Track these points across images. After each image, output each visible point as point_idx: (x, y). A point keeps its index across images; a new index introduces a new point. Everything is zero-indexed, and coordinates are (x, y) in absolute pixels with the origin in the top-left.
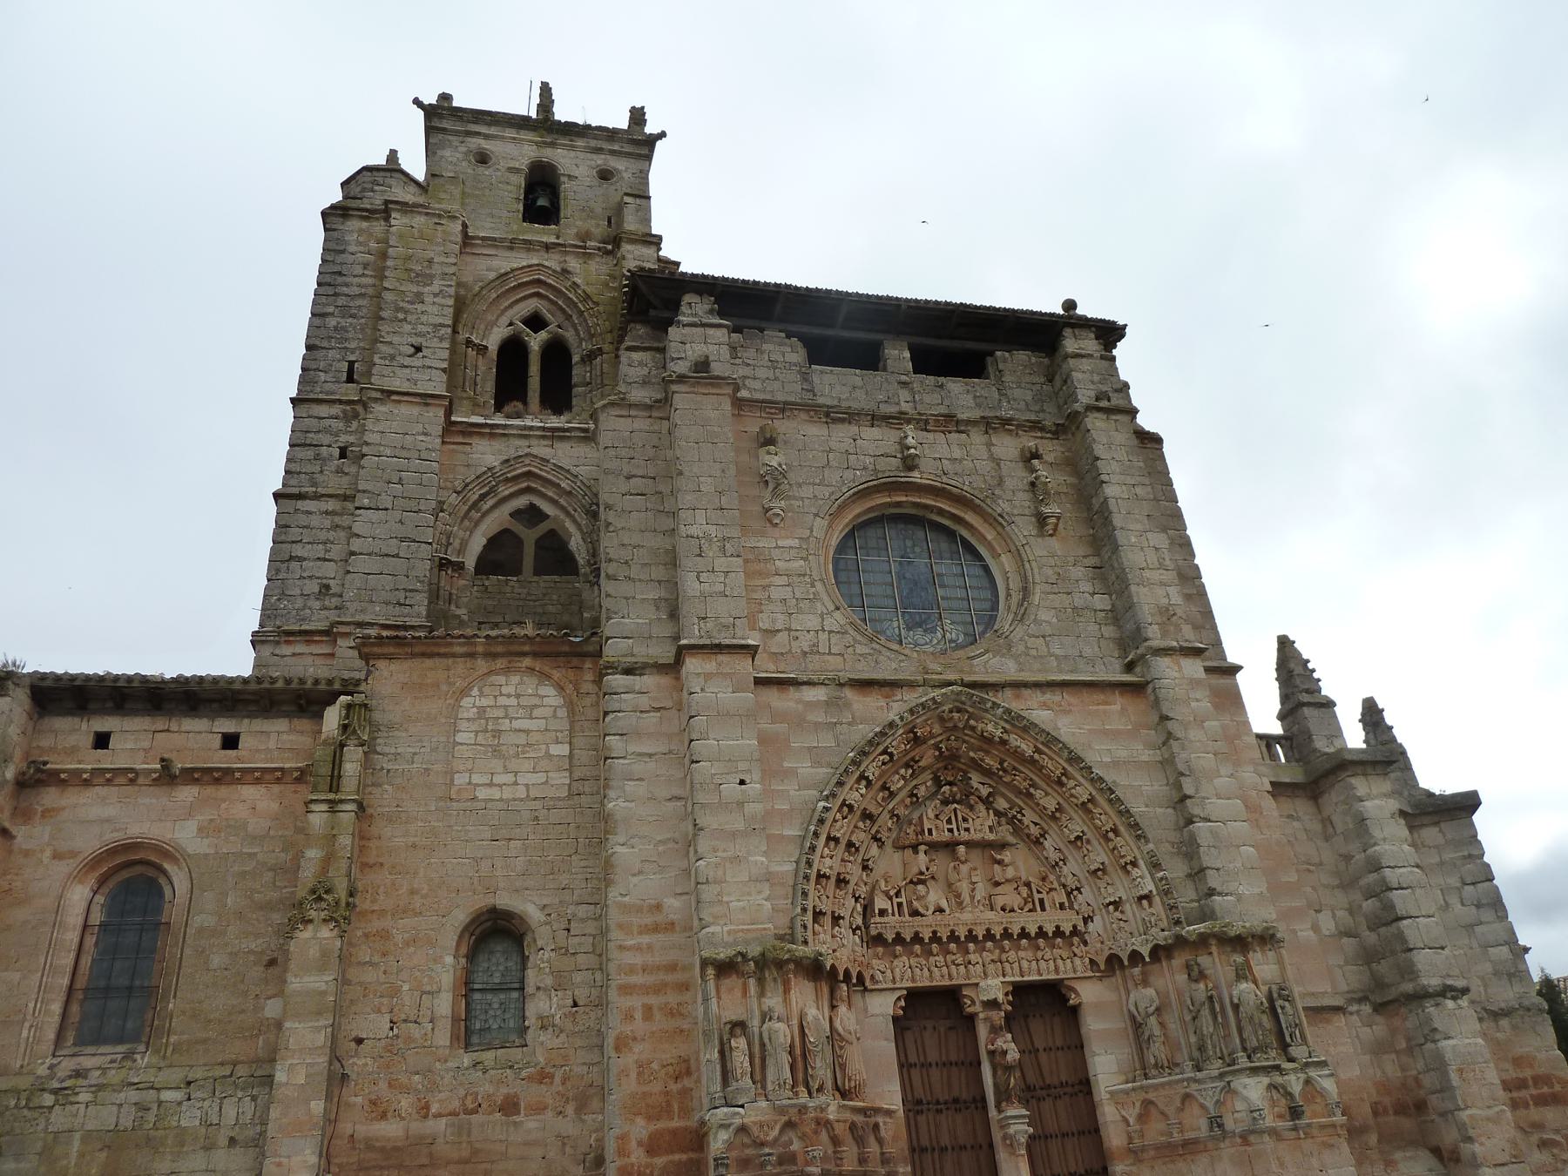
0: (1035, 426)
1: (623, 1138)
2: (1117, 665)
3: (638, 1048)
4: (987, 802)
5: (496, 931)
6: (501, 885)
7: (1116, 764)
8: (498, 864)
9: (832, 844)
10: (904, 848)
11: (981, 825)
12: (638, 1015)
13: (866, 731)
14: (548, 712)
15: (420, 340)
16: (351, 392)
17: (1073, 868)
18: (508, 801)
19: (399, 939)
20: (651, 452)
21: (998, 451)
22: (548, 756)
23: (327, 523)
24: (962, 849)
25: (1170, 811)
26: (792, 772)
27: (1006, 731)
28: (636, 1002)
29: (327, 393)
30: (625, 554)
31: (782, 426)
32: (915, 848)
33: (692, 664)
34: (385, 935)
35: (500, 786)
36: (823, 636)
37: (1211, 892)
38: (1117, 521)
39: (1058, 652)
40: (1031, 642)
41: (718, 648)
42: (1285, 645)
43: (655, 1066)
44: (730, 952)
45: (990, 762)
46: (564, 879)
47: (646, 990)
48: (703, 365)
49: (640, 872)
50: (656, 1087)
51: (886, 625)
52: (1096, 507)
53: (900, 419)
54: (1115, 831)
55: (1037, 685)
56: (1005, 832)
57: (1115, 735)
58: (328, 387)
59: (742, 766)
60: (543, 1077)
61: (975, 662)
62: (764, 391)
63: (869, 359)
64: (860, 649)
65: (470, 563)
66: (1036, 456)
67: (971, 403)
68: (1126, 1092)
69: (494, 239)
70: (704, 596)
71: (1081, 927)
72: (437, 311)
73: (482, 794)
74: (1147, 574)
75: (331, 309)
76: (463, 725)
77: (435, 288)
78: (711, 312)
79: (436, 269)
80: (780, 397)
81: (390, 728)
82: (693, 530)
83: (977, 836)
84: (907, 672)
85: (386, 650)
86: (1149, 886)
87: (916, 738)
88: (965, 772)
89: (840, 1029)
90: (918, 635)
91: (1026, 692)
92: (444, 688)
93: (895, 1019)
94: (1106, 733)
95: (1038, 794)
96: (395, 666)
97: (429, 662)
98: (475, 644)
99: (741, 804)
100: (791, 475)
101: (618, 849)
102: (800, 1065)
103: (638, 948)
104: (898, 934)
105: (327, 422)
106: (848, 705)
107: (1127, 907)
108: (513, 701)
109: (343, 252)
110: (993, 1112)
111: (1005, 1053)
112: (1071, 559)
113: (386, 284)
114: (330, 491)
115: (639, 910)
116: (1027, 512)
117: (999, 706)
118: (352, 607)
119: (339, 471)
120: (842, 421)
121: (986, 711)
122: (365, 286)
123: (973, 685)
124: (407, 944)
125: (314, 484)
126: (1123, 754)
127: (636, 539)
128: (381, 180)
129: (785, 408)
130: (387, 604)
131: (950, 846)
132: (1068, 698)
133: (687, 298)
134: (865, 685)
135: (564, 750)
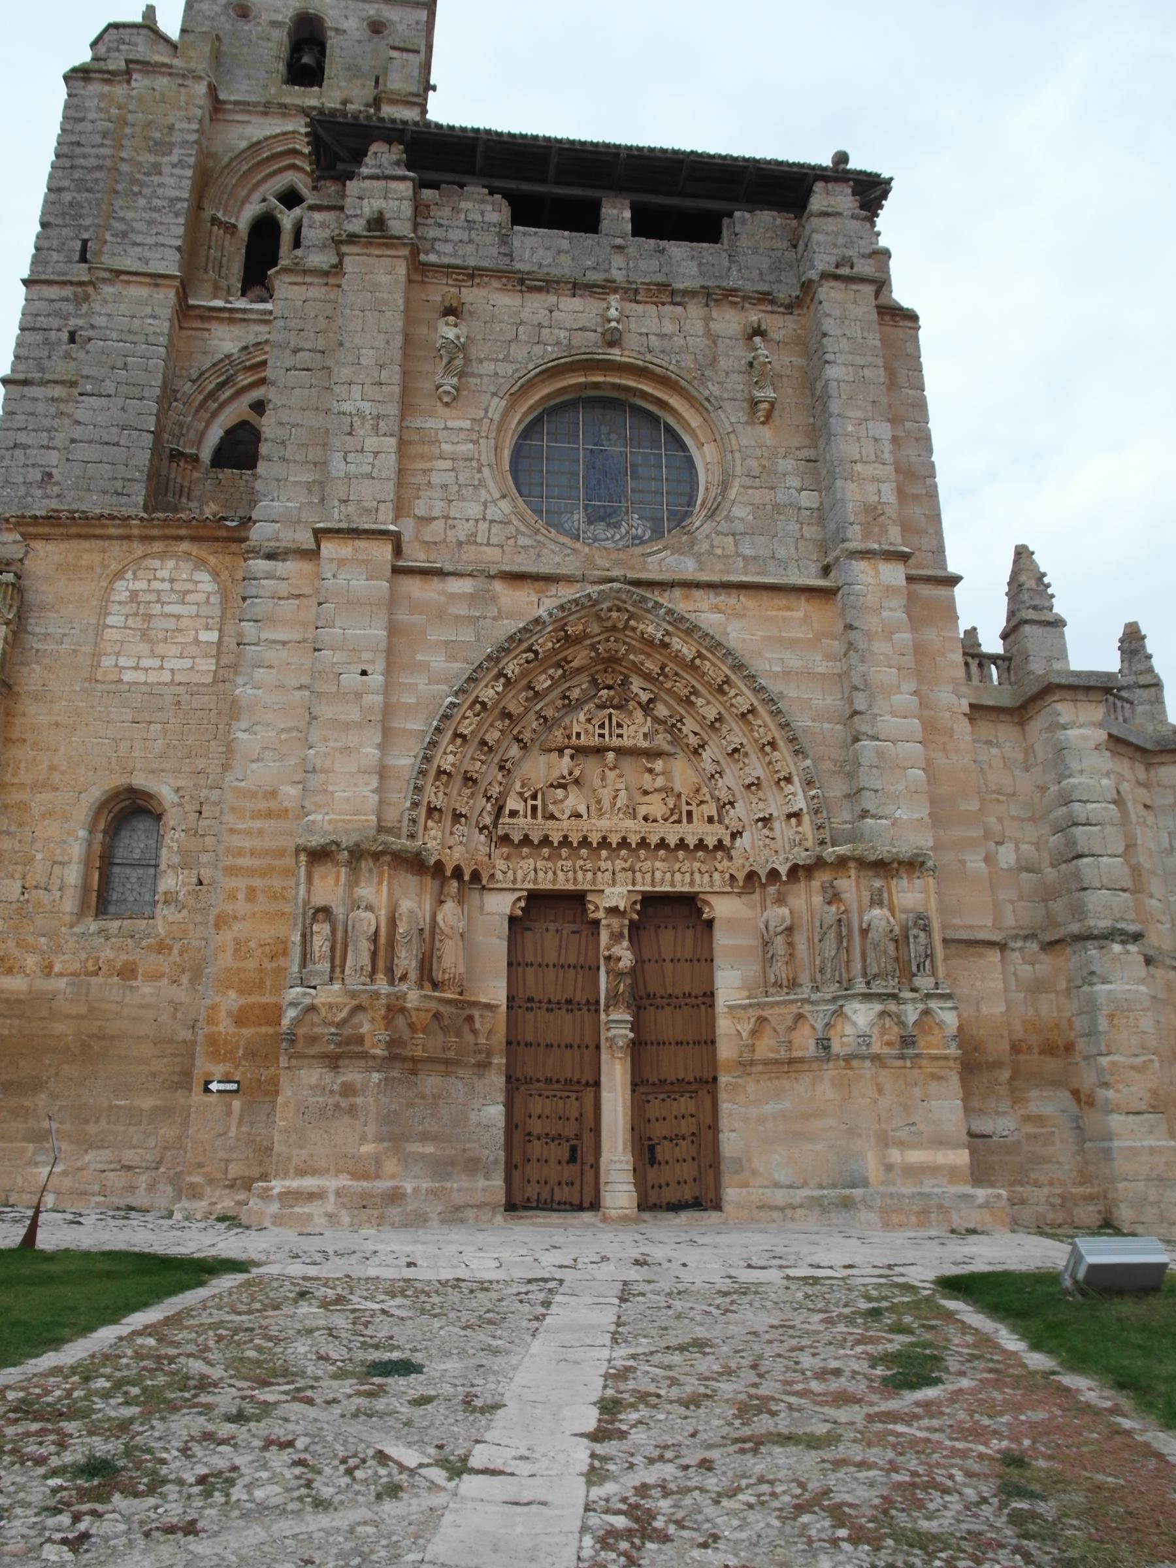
0: (765, 298)
1: (214, 1007)
2: (814, 569)
3: (237, 927)
4: (647, 708)
5: (129, 810)
6: (138, 766)
7: (787, 674)
8: (137, 745)
9: (459, 741)
10: (550, 751)
11: (635, 731)
12: (241, 896)
13: (511, 626)
14: (201, 597)
15: (155, 215)
16: (80, 272)
17: (731, 780)
18: (152, 685)
19: (36, 811)
20: (322, 323)
21: (717, 327)
22: (197, 641)
23: (53, 410)
24: (611, 755)
25: (839, 727)
26: (425, 666)
27: (668, 633)
28: (241, 883)
29: (59, 274)
30: (282, 433)
31: (472, 295)
32: (561, 751)
33: (329, 548)
34: (23, 807)
35: (146, 670)
36: (483, 526)
37: (865, 814)
38: (835, 406)
39: (747, 552)
40: (718, 540)
41: (355, 533)
42: (1022, 554)
43: (252, 944)
44: (322, 841)
45: (651, 666)
46: (201, 763)
47: (252, 872)
48: (378, 223)
49: (258, 760)
50: (251, 964)
51: (565, 517)
52: (818, 392)
53: (605, 288)
54: (773, 744)
55: (710, 586)
56: (661, 740)
57: (792, 643)
58: (61, 267)
59: (366, 656)
60: (162, 947)
61: (650, 559)
62: (455, 255)
63: (583, 219)
64: (522, 541)
65: (206, 455)
66: (758, 332)
67: (695, 270)
68: (744, 1007)
69: (248, 104)
70: (348, 477)
71: (727, 841)
72: (176, 183)
73: (128, 676)
74: (858, 467)
75: (66, 183)
76: (114, 608)
77: (174, 158)
78: (398, 163)
79: (177, 137)
80: (472, 262)
81: (42, 608)
82: (347, 407)
83: (627, 742)
84: (571, 566)
85: (41, 530)
86: (800, 803)
87: (567, 637)
88: (626, 677)
89: (441, 923)
90: (599, 529)
91: (698, 594)
92: (98, 570)
93: (512, 920)
94: (780, 641)
95: (700, 702)
96: (51, 547)
97: (86, 544)
98: (130, 527)
99: (358, 695)
100: (474, 351)
101: (240, 735)
102: (382, 953)
103: (249, 832)
104: (526, 836)
105: (57, 305)
106: (495, 599)
107: (776, 825)
108: (166, 586)
109: (82, 120)
110: (603, 1016)
111: (619, 959)
112: (782, 451)
113: (123, 154)
114: (56, 377)
115: (253, 795)
116: (739, 396)
117: (661, 606)
118: (70, 494)
119: (67, 356)
120: (539, 289)
121: (648, 611)
122: (104, 157)
123: (638, 583)
124: (43, 816)
125: (42, 370)
126: (794, 662)
127: (295, 417)
128: (127, 38)
129: (473, 275)
130: (105, 492)
131: (600, 751)
132: (745, 601)
133: (375, 147)
134: (517, 578)
135: (213, 636)
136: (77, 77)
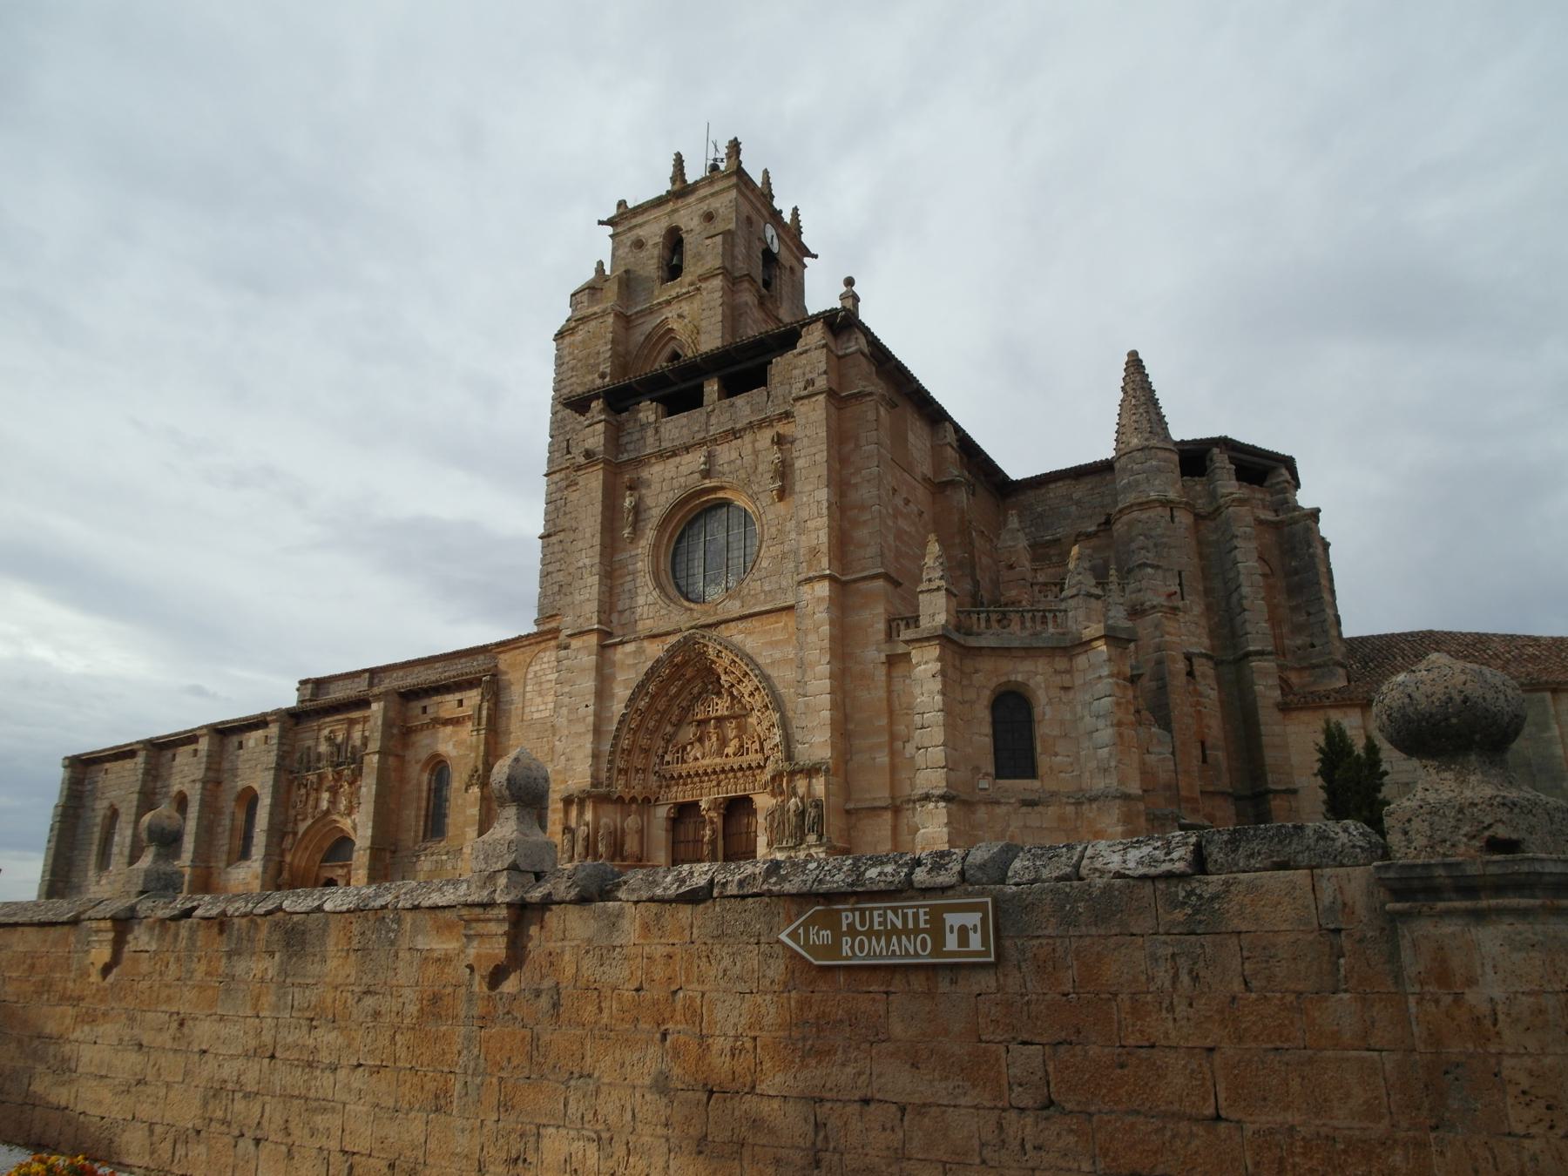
91: (732, 624)
126: (778, 655)
136: (560, 336)
